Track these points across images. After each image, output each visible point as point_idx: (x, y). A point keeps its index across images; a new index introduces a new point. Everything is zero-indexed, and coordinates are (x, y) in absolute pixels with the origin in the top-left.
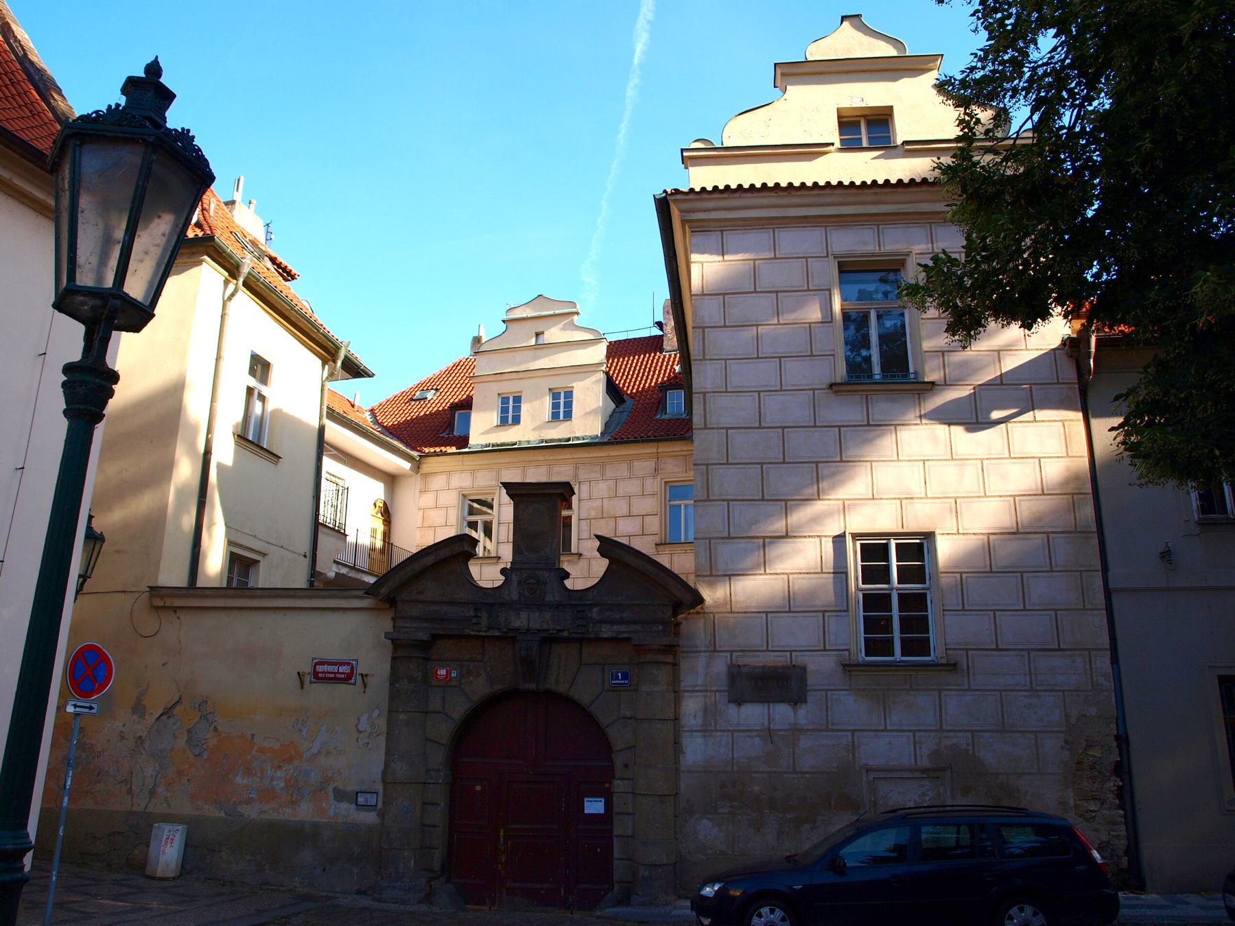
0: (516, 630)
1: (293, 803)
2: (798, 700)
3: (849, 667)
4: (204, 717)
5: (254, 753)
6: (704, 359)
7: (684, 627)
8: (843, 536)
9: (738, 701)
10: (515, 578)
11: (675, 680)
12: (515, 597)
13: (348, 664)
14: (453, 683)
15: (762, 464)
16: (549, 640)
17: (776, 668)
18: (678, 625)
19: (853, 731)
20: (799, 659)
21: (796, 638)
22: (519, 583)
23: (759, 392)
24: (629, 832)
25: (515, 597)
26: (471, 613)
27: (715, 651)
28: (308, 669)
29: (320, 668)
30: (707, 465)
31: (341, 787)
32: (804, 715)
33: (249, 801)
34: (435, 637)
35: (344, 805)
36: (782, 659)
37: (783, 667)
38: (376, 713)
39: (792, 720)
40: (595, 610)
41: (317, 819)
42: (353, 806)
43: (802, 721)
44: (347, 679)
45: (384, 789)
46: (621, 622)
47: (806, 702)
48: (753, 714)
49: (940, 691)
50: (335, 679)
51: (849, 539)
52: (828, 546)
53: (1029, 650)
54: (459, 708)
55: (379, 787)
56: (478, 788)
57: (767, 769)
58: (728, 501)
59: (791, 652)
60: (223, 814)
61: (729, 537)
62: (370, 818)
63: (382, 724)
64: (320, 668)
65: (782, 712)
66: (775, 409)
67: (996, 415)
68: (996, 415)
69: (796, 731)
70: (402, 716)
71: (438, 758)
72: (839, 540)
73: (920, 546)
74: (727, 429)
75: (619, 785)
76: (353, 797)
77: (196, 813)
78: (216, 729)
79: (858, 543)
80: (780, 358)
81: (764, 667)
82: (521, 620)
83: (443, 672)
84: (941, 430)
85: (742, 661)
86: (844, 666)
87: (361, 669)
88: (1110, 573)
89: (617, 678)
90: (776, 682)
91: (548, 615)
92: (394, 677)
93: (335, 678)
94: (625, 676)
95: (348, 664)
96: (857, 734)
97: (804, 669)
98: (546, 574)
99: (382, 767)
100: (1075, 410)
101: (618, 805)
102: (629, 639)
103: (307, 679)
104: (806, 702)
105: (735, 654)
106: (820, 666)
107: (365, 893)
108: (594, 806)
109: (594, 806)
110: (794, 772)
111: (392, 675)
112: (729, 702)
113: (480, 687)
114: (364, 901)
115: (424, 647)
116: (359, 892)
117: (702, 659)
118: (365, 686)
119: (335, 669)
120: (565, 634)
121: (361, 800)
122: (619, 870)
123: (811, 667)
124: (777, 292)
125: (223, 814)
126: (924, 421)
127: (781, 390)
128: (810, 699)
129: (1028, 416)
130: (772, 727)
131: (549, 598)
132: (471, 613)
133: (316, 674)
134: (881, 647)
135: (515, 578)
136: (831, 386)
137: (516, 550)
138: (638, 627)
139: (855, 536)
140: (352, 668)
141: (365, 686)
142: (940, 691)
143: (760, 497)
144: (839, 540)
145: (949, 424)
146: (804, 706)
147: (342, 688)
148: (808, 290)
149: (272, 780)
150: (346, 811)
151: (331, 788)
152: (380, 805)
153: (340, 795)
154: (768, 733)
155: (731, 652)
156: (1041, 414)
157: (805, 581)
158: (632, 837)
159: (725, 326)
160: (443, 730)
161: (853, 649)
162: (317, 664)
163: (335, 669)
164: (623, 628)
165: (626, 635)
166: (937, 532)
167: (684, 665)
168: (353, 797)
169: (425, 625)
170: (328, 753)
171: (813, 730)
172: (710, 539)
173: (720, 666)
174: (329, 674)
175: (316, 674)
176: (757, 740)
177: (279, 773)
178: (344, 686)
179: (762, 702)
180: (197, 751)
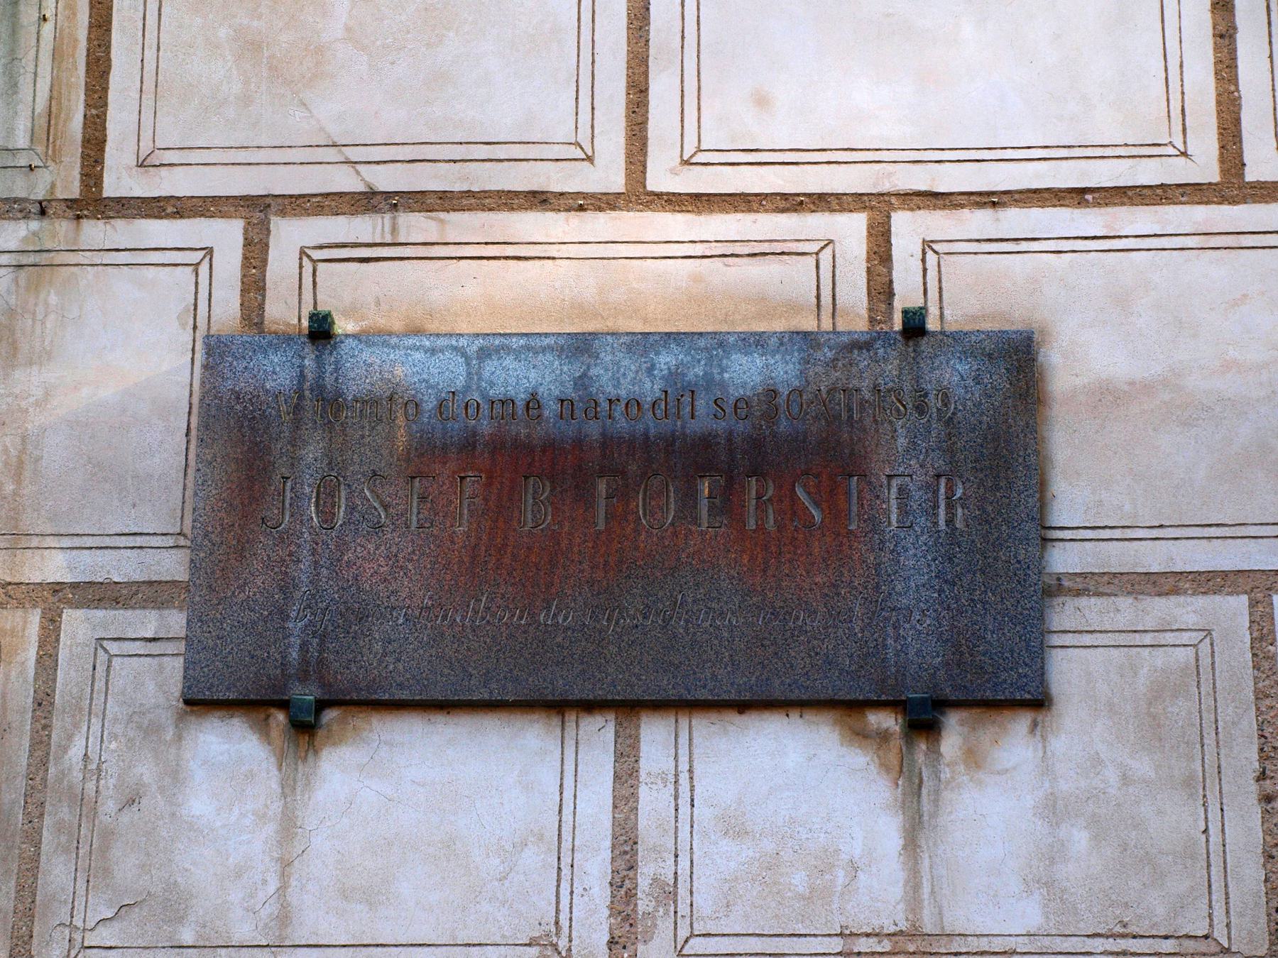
9: (290, 687)
20: (968, 278)
27: (92, 203)
36: (795, 279)
39: (879, 899)
47: (1022, 694)
59: (878, 207)
97: (1016, 360)
105: (289, 235)
112: (199, 703)
123: (1081, 359)
128: (1069, 670)
146: (1014, 744)
155: (258, 211)
179: (560, 707)
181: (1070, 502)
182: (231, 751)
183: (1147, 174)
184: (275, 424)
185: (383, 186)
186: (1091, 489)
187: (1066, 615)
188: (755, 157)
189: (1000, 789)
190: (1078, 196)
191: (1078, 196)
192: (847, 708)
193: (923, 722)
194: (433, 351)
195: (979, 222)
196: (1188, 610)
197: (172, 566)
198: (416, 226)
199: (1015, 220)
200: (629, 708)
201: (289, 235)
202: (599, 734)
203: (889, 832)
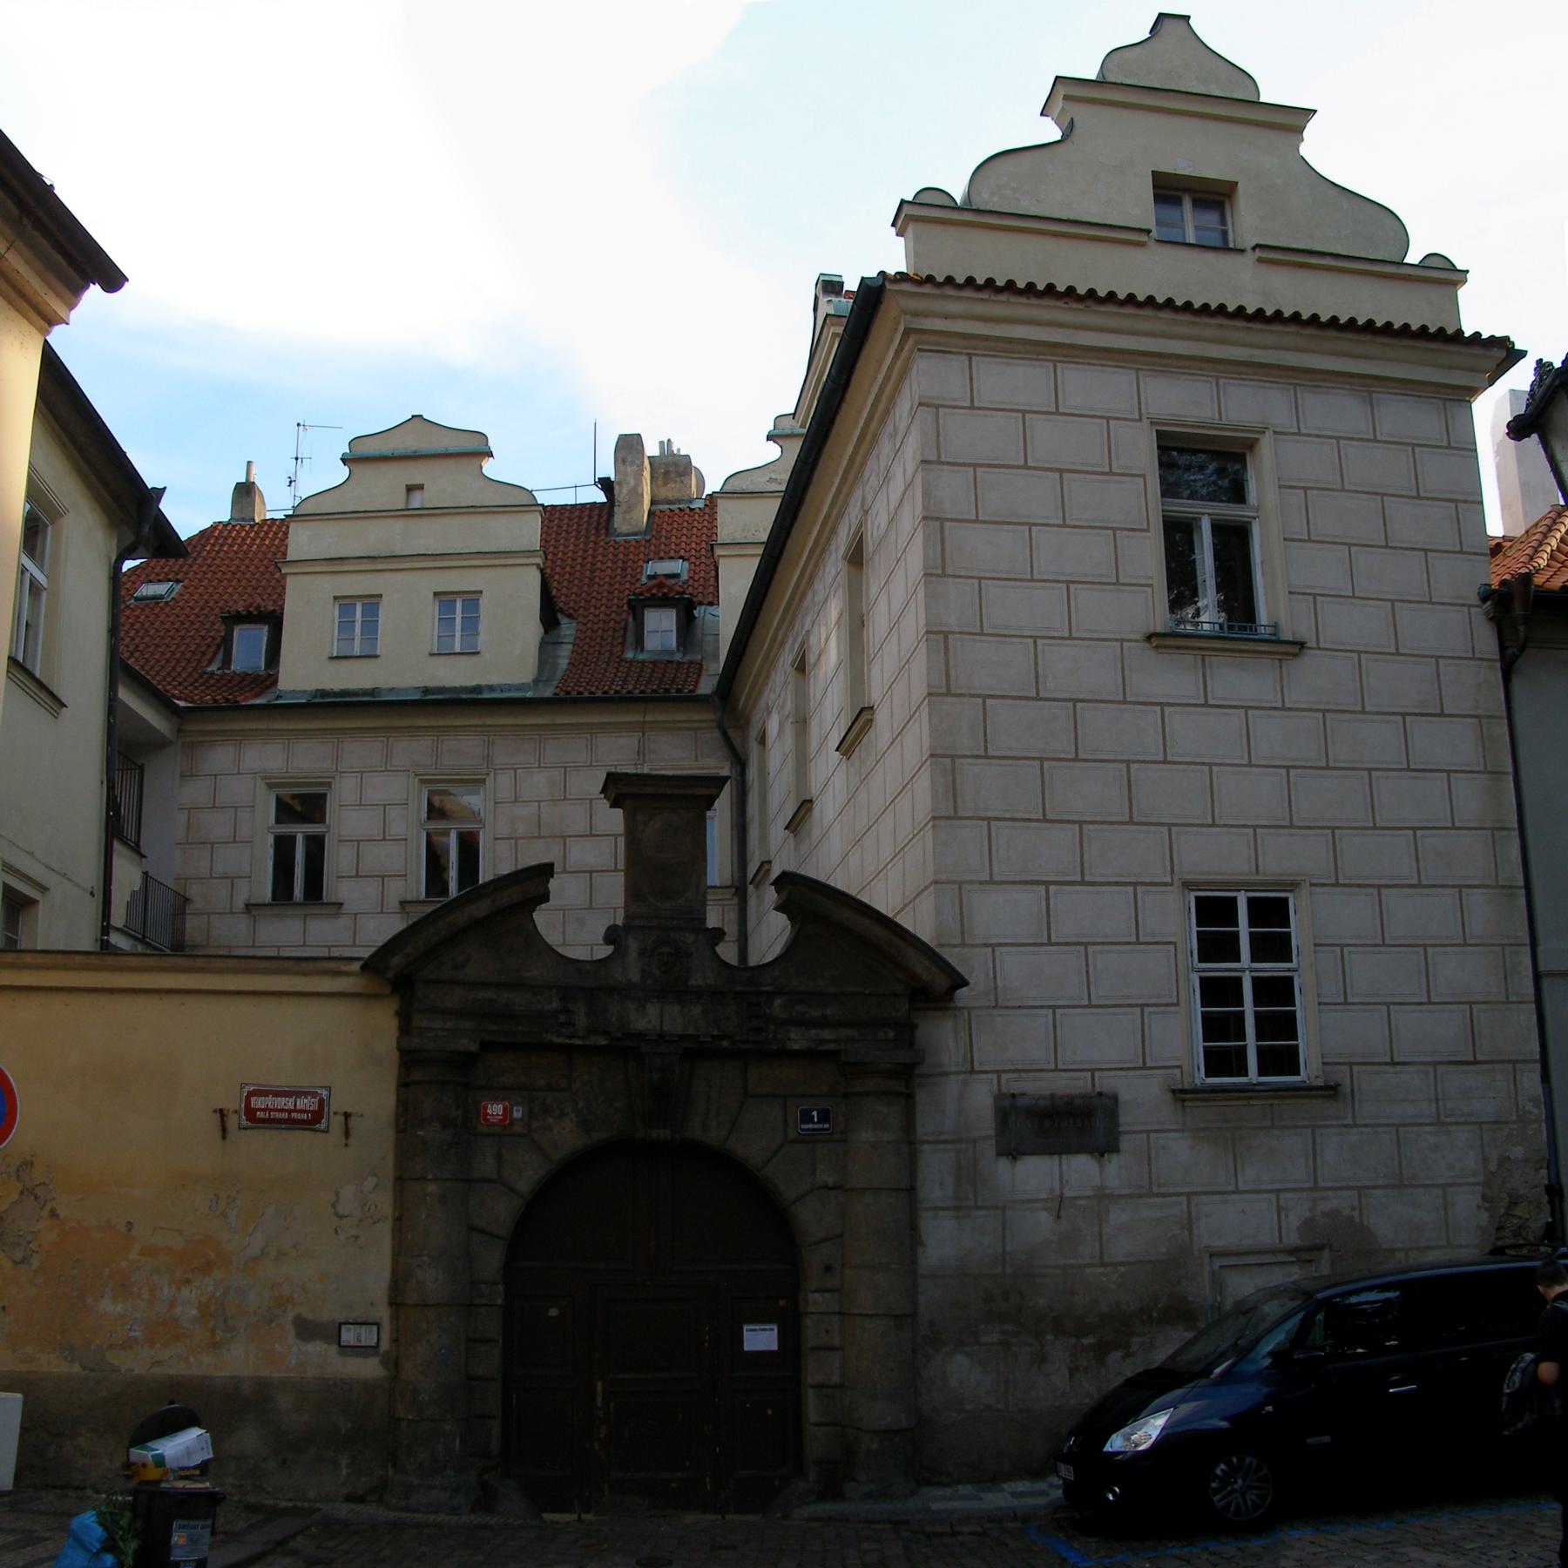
0: (641, 1035)
1: (216, 1345)
3: (1182, 1095)
4: (29, 1192)
5: (133, 1256)
6: (944, 575)
7: (921, 1034)
9: (1012, 1151)
10: (633, 945)
11: (909, 1124)
12: (635, 976)
13: (314, 1094)
14: (517, 1129)
15: (1042, 760)
16: (696, 1052)
17: (1071, 1097)
18: (913, 1027)
19: (1189, 1195)
20: (1106, 1083)
22: (642, 953)
23: (1035, 639)
24: (836, 1379)
25: (635, 976)
26: (555, 1004)
27: (972, 1072)
28: (233, 1103)
29: (257, 1102)
30: (953, 757)
31: (309, 1316)
32: (1115, 1171)
33: (129, 1344)
34: (486, 1046)
35: (316, 1348)
37: (1083, 1096)
38: (371, 1182)
40: (778, 1002)
41: (264, 1373)
42: (333, 1348)
44: (312, 1121)
45: (395, 1317)
46: (824, 1023)
47: (1118, 1151)
48: (1036, 1174)
50: (291, 1123)
54: (527, 1173)
55: (383, 1313)
56: (554, 1312)
57: (1062, 1262)
58: (989, 819)
59: (1093, 1071)
60: (76, 1369)
61: (991, 882)
62: (369, 1369)
63: (384, 1202)
64: (257, 1102)
65: (1081, 1169)
69: (1104, 1197)
70: (432, 1188)
71: (491, 1259)
74: (985, 697)
75: (816, 1302)
76: (330, 1332)
77: (23, 1368)
78: (54, 1214)
79: (1192, 896)
80: (1068, 583)
81: (1052, 1096)
82: (648, 1018)
83: (496, 1109)
85: (1017, 1087)
87: (338, 1103)
88: (1540, 949)
89: (806, 1118)
90: (1071, 1122)
91: (696, 1010)
92: (406, 1118)
93: (291, 1121)
94: (824, 1116)
95: (314, 1094)
96: (1195, 1199)
98: (690, 938)
99: (387, 1275)
101: (813, 1331)
102: (834, 1054)
103: (232, 1122)
104: (1118, 1151)
105: (1005, 1077)
107: (361, 1500)
108: (760, 1338)
109: (760, 1338)
110: (1103, 1264)
111: (398, 1116)
112: (999, 1154)
113: (566, 1136)
114: (371, 1511)
115: (464, 1063)
116: (351, 1498)
117: (952, 1086)
118: (347, 1133)
119: (289, 1103)
120: (725, 1043)
121: (348, 1336)
122: (817, 1441)
123: (1124, 1096)
124: (1061, 471)
125: (76, 1369)
127: (1070, 638)
128: (1123, 1146)
130: (1067, 1193)
131: (696, 980)
132: (555, 1004)
133: (250, 1113)
134: (1222, 1061)
135: (633, 945)
136: (1149, 638)
137: (634, 892)
138: (852, 1033)
140: (321, 1102)
141: (347, 1133)
146: (1114, 1158)
147: (302, 1137)
148: (1111, 473)
149: (172, 1305)
150: (320, 1359)
151: (290, 1316)
152: (385, 1345)
153: (307, 1330)
154: (1060, 1205)
155: (999, 1073)
158: (841, 1386)
159: (977, 521)
160: (500, 1211)
162: (250, 1094)
163: (289, 1103)
164: (827, 1034)
165: (831, 1047)
167: (921, 1097)
168: (330, 1332)
169: (468, 1025)
170: (281, 1255)
171: (1130, 1196)
172: (960, 883)
173: (982, 1099)
174: (259, 1114)
175: (250, 1113)
176: (1044, 1214)
177: (185, 1292)
178: (307, 1133)
179: (1050, 1154)
180: (19, 1254)
181: (1122, 1120)
182: (1004, 1163)
184: (1009, 1110)
189: (1114, 1164)
196: (1139, 1136)
197: (992, 1133)
200: (1061, 1153)
201: (1005, 1077)
202: (1056, 1157)
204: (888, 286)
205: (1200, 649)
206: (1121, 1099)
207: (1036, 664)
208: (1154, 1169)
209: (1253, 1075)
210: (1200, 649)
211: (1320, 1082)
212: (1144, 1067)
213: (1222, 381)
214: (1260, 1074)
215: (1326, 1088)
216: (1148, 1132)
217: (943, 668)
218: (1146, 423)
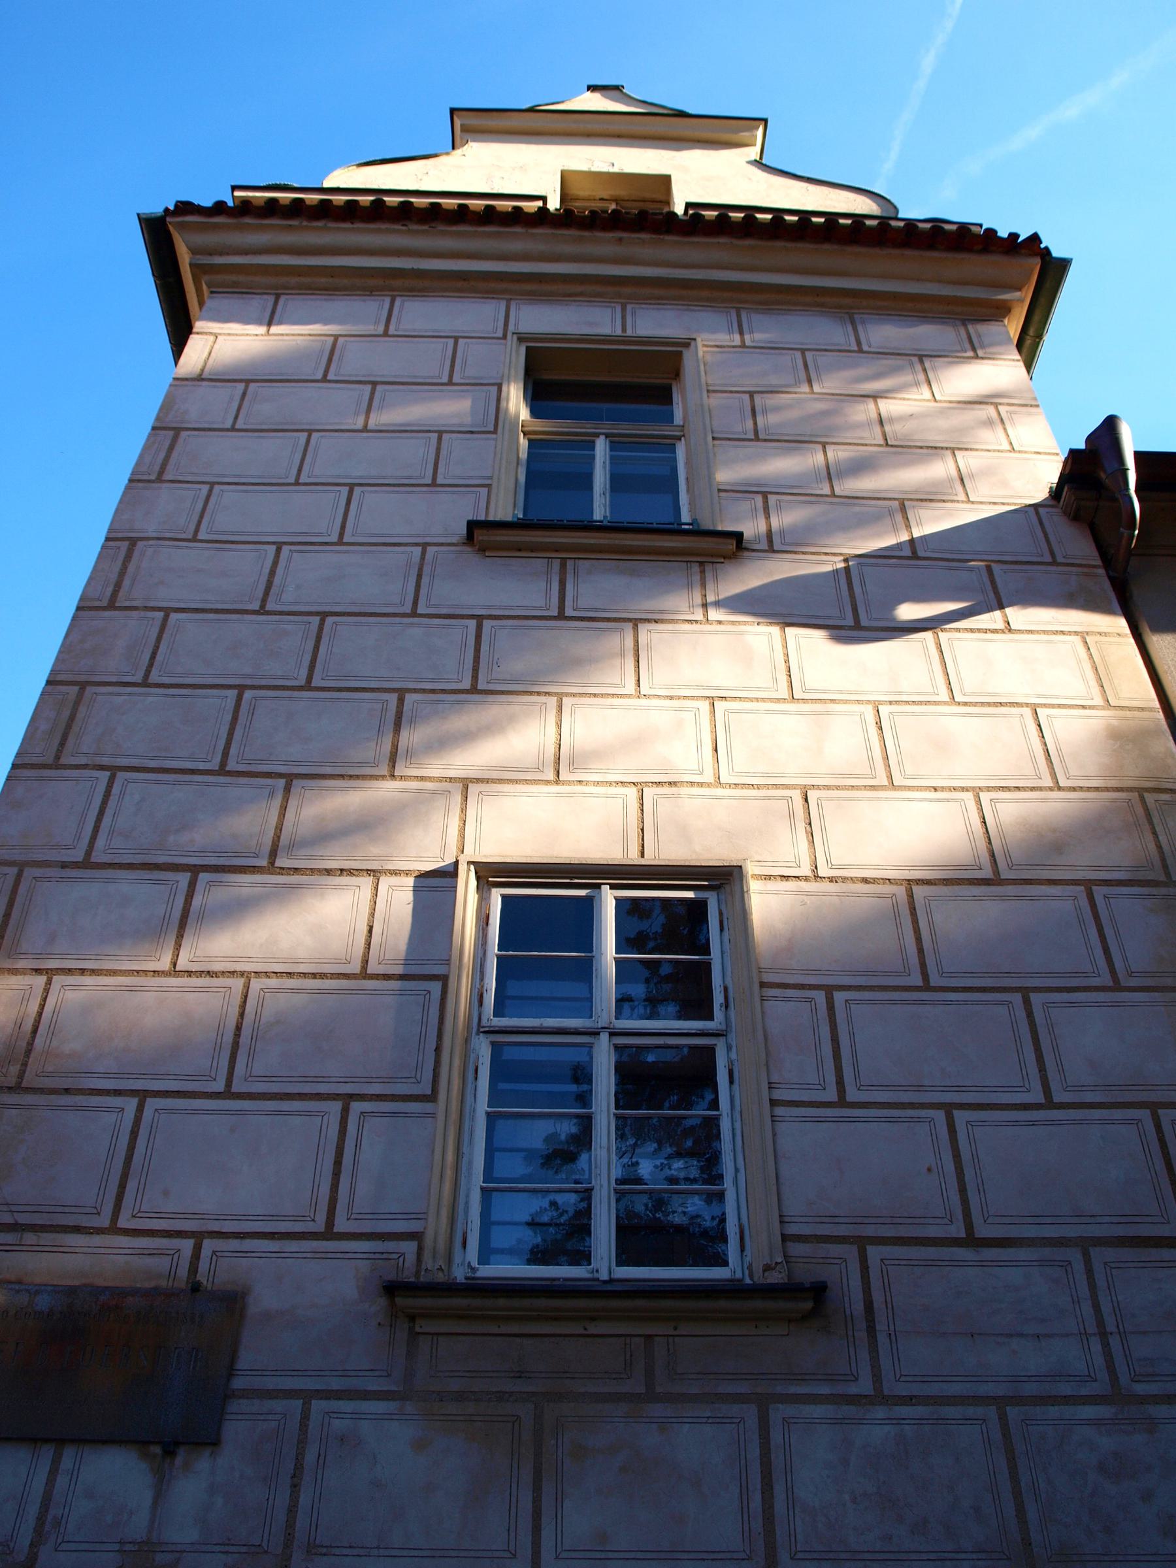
2: (177, 1429)
3: (413, 1298)
8: (449, 873)
20: (224, 1266)
21: (229, 1184)
36: (163, 1264)
43: (181, 1531)
49: (764, 1402)
51: (467, 884)
52: (398, 900)
53: (1086, 1244)
59: (199, 1237)
66: (306, 579)
67: (908, 612)
68: (908, 612)
72: (436, 885)
73: (697, 910)
79: (496, 898)
84: (762, 637)
86: (392, 1289)
100: (1106, 610)
106: (308, 1296)
126: (714, 614)
129: (992, 619)
139: (490, 874)
142: (764, 1402)
143: (214, 764)
144: (436, 885)
145: (787, 622)
146: (203, 1462)
156: (1018, 615)
157: (298, 999)
161: (436, 1229)
166: (751, 869)
181: (244, 1361)
183: (298, 1227)
185: (20, 1221)
186: (253, 1354)
187: (234, 1406)
188: (159, 1215)
190: (272, 1236)
191: (272, 1236)
192: (141, 1443)
193: (170, 1451)
194: (18, 1291)
195: (234, 1244)
198: (30, 1238)
199: (248, 1244)
203: (148, 1496)
204: (168, 219)
205: (557, 548)
206: (253, 1309)
207: (272, 573)
208: (304, 1499)
209: (604, 1257)
210: (557, 548)
211: (775, 1278)
212: (329, 1233)
213: (629, 307)
214: (625, 1256)
215: (791, 1290)
216: (307, 1396)
217: (114, 577)
218: (512, 340)
